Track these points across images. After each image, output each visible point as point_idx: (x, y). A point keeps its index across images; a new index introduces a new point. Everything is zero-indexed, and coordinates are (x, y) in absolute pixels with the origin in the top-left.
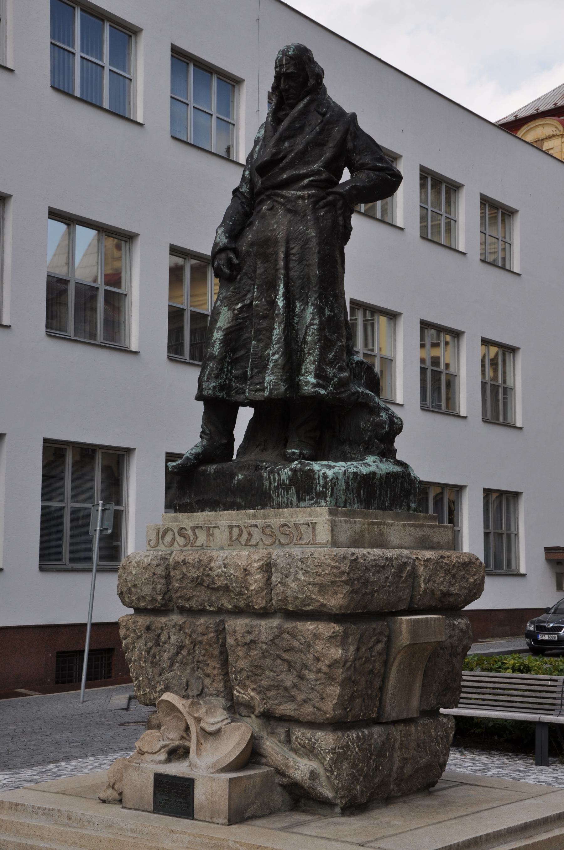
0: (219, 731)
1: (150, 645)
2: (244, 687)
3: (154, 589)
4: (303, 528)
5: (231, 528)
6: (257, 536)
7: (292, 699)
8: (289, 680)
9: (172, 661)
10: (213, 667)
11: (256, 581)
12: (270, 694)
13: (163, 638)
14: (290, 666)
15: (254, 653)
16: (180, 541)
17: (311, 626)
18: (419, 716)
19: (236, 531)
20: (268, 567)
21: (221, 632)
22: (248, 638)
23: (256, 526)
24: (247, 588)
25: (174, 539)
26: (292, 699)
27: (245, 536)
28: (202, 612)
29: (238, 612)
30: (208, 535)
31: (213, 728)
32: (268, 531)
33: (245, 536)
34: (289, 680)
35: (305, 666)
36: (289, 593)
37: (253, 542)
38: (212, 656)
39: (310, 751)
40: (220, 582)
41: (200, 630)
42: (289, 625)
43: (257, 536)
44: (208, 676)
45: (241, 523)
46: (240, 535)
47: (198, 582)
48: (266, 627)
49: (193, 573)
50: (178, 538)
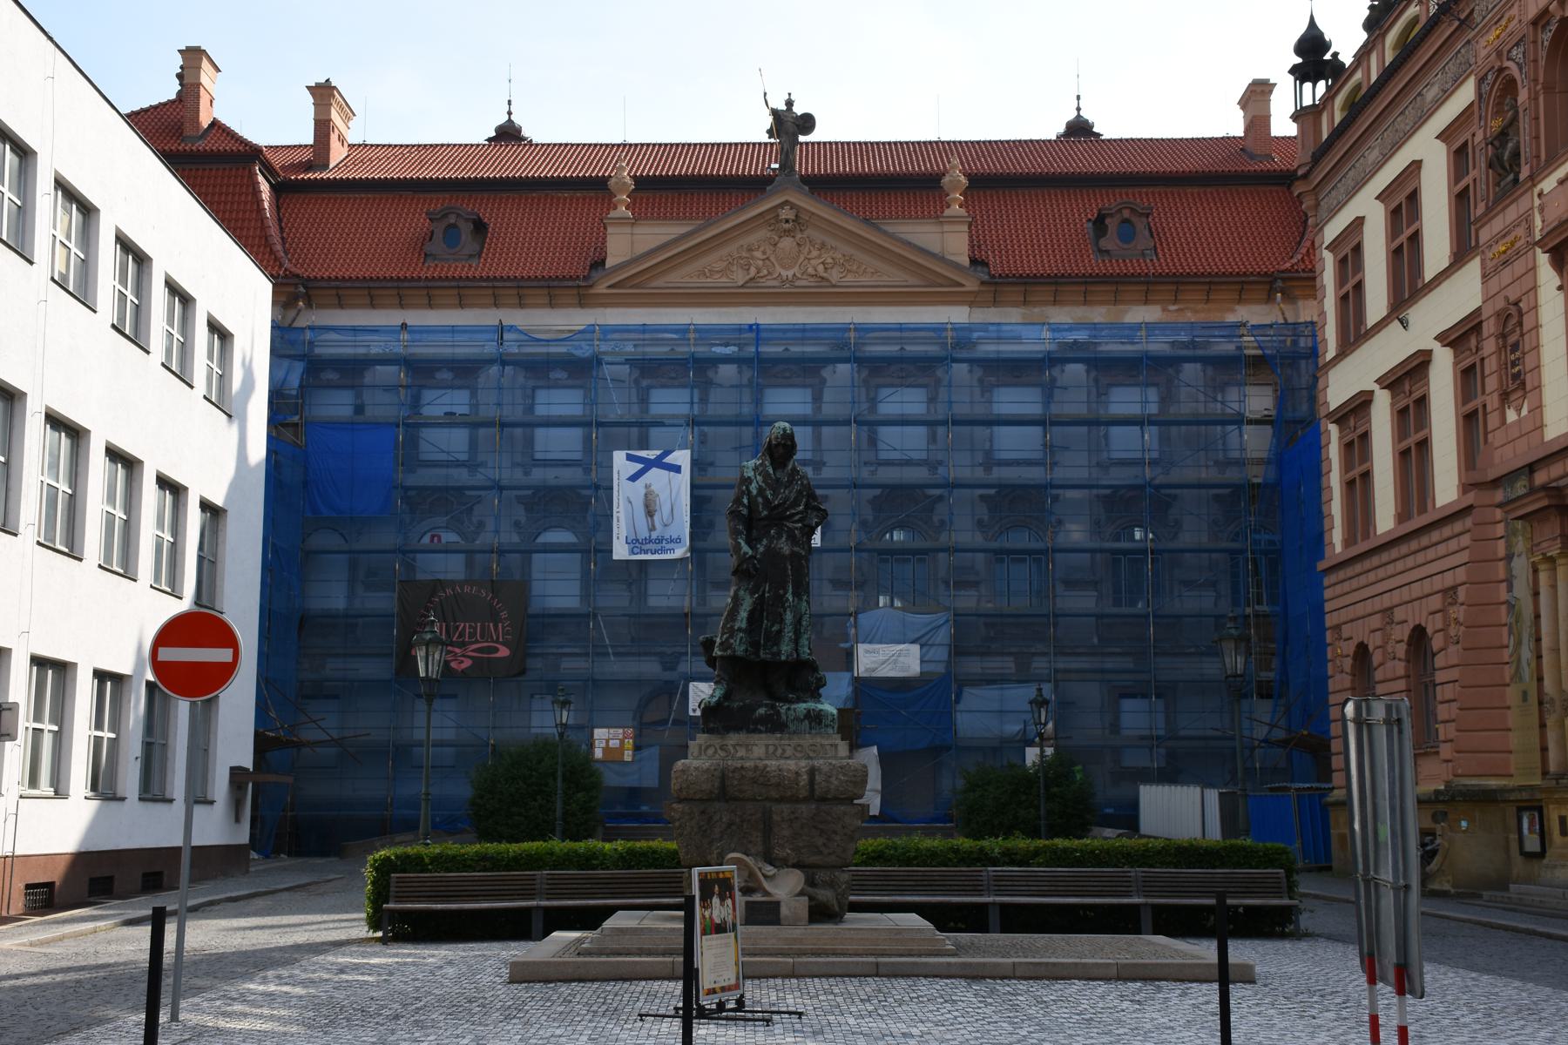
5: (767, 746)
7: (821, 853)
8: (820, 841)
13: (716, 818)
16: (723, 754)
18: (243, 836)
19: (771, 749)
20: (812, 772)
26: (821, 853)
27: (779, 751)
29: (781, 800)
33: (779, 751)
34: (820, 841)
35: (835, 832)
39: (831, 884)
40: (773, 781)
43: (789, 752)
47: (754, 781)
48: (805, 810)
49: (750, 774)
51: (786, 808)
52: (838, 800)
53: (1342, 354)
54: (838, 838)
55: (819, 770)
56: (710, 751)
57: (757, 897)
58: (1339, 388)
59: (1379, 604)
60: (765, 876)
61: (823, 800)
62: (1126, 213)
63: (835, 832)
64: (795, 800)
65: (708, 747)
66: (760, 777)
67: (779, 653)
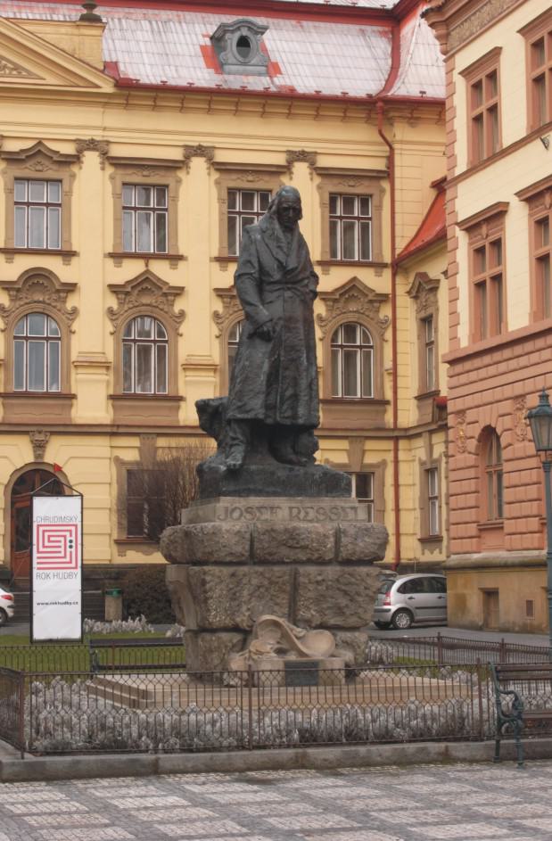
0: (304, 636)
1: (231, 586)
2: (309, 609)
3: (244, 548)
4: (348, 510)
5: (291, 508)
6: (312, 514)
8: (343, 601)
9: (251, 595)
10: (284, 599)
11: (330, 544)
12: (327, 612)
13: (244, 581)
14: (346, 593)
15: (320, 588)
16: (248, 516)
17: (364, 570)
19: (295, 511)
20: (338, 534)
21: (295, 575)
22: (319, 578)
23: (312, 508)
24: (325, 547)
25: (241, 515)
27: (302, 515)
28: (281, 563)
29: (309, 562)
30: (272, 512)
31: (301, 635)
32: (321, 511)
33: (302, 515)
34: (343, 601)
35: (358, 594)
36: (357, 549)
37: (309, 518)
38: (284, 591)
41: (277, 574)
42: (347, 569)
43: (312, 514)
44: (277, 604)
45: (298, 505)
46: (299, 513)
48: (331, 571)
50: (245, 514)
51: (312, 569)
52: (360, 562)
53: (473, 170)
54: (360, 599)
55: (345, 532)
56: (236, 514)
57: (292, 657)
58: (469, 201)
59: (509, 391)
60: (297, 638)
61: (348, 562)
62: (245, 32)
63: (358, 594)
64: (321, 562)
65: (233, 510)
66: (291, 539)
67: (295, 416)
